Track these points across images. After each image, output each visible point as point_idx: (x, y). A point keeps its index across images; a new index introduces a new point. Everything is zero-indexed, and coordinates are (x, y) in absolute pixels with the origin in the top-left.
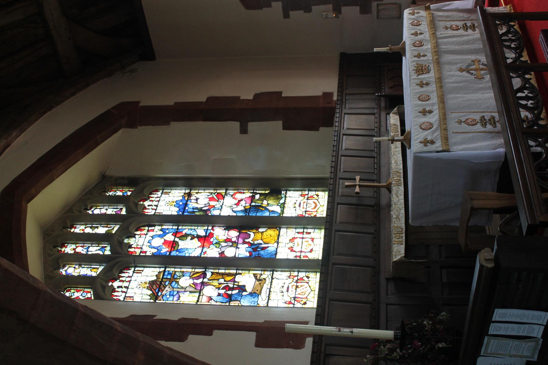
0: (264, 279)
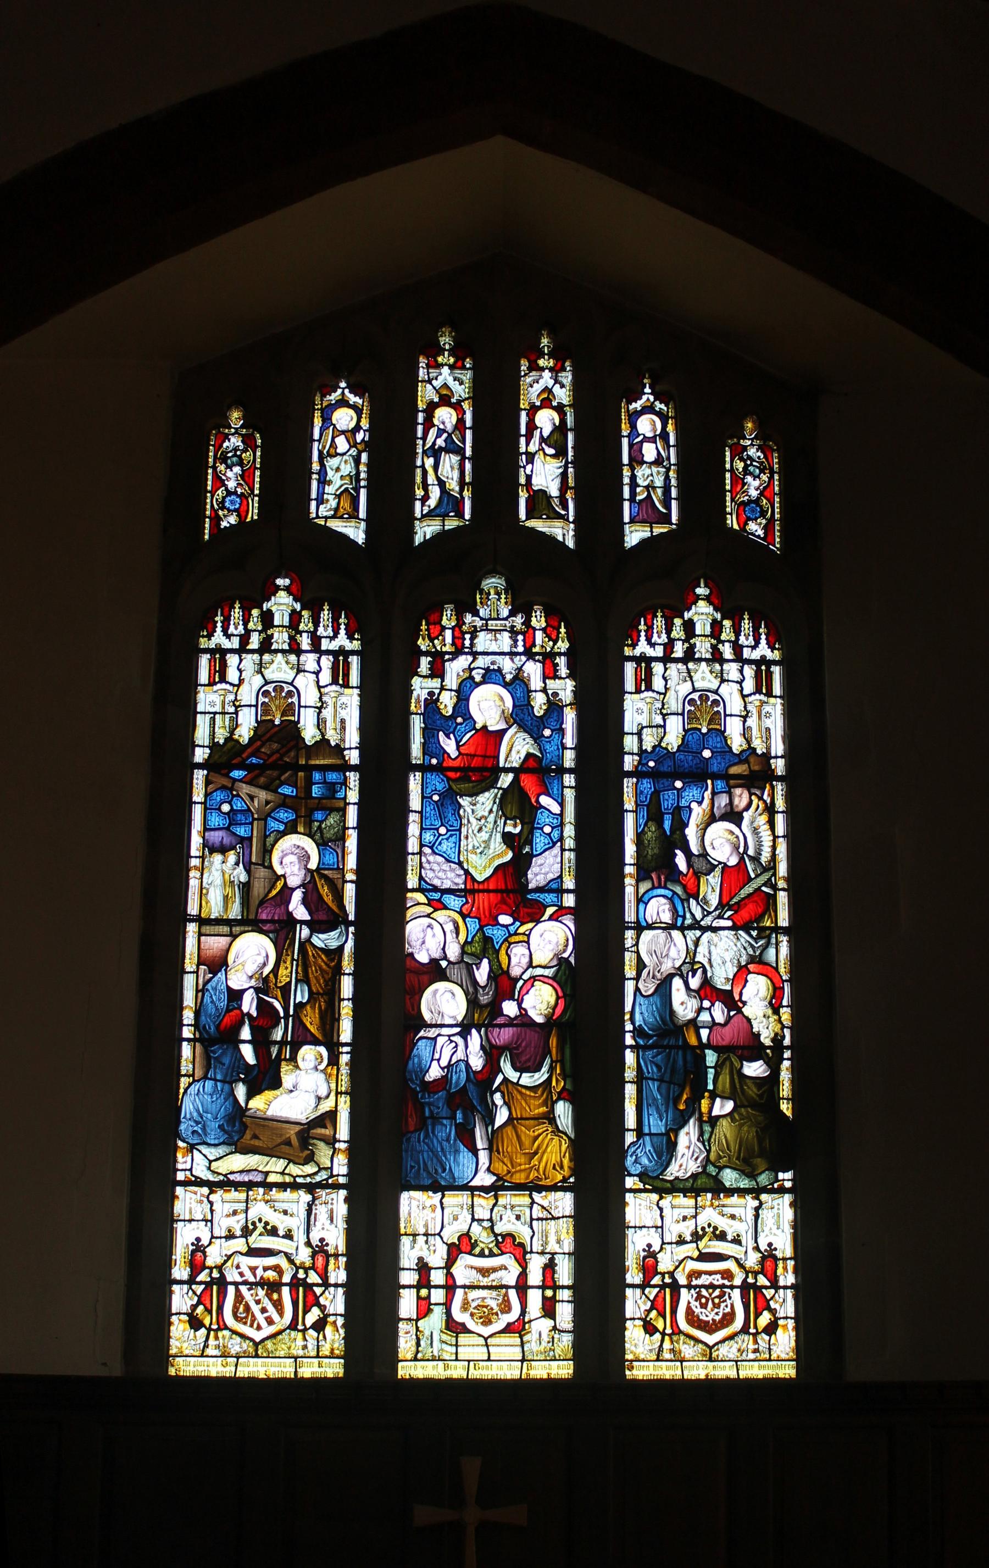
0: (313, 1153)
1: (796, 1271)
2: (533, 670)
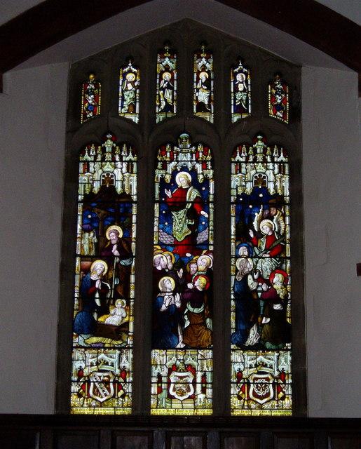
1: (292, 378)
2: (199, 167)
